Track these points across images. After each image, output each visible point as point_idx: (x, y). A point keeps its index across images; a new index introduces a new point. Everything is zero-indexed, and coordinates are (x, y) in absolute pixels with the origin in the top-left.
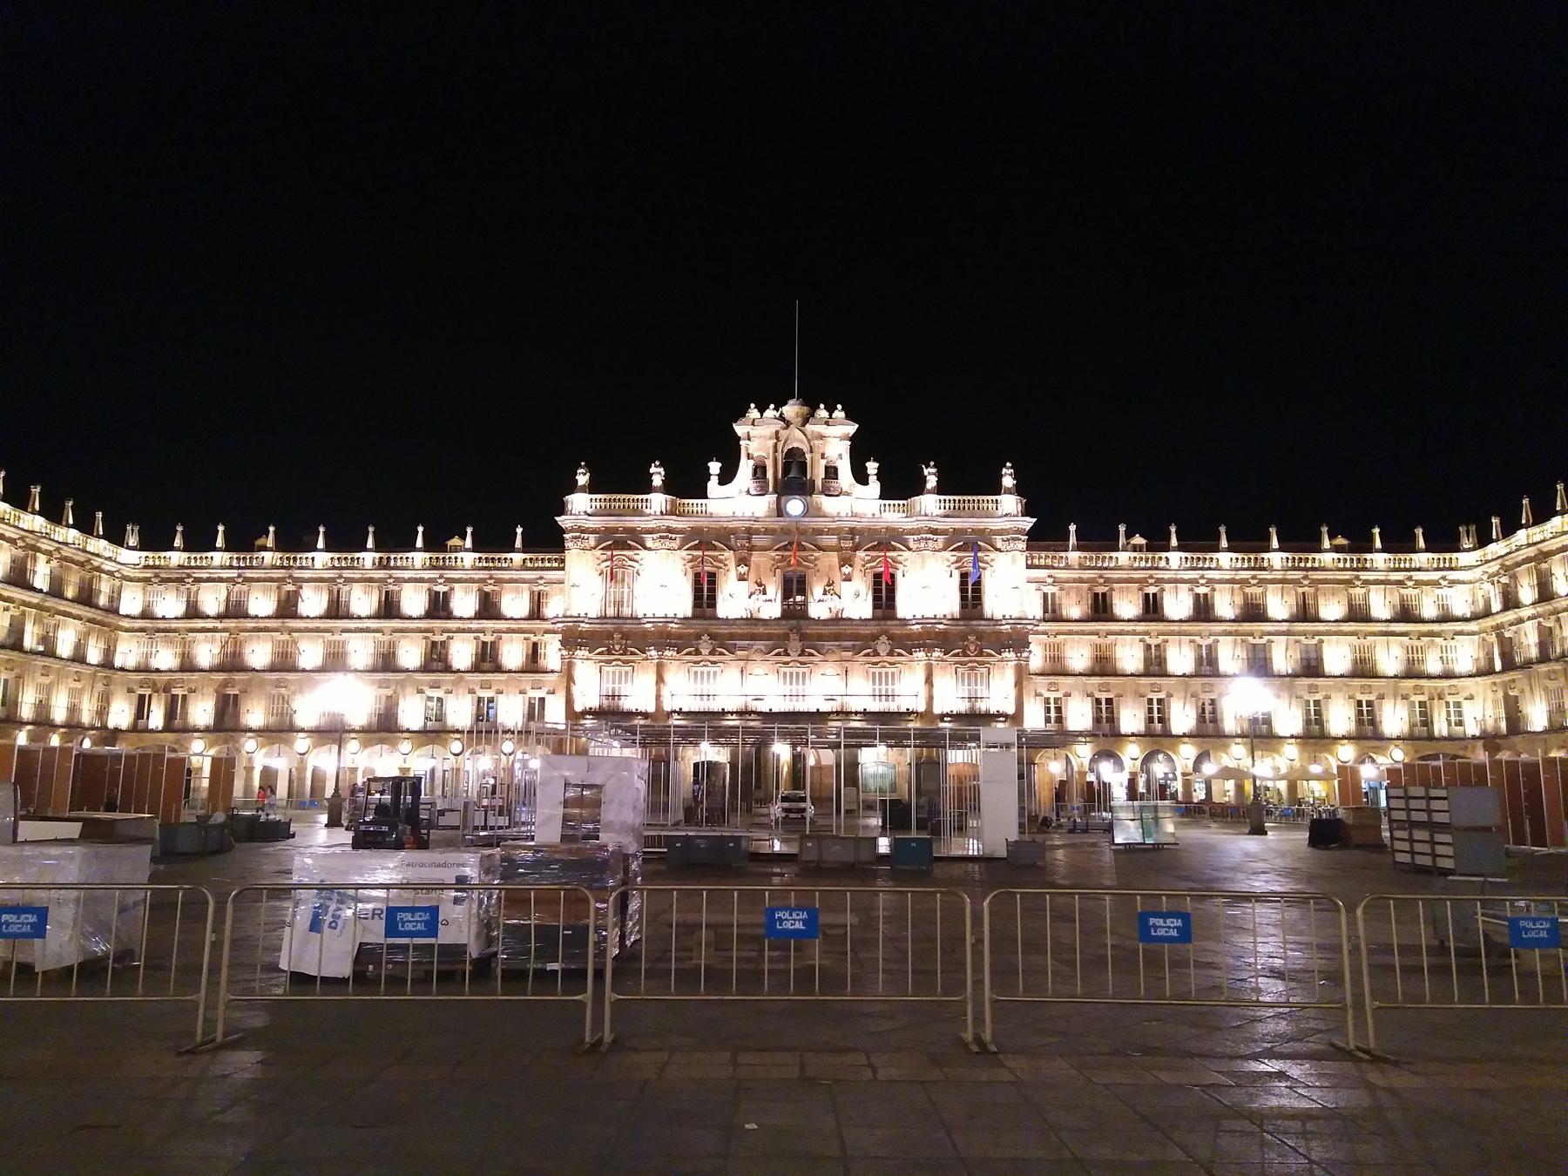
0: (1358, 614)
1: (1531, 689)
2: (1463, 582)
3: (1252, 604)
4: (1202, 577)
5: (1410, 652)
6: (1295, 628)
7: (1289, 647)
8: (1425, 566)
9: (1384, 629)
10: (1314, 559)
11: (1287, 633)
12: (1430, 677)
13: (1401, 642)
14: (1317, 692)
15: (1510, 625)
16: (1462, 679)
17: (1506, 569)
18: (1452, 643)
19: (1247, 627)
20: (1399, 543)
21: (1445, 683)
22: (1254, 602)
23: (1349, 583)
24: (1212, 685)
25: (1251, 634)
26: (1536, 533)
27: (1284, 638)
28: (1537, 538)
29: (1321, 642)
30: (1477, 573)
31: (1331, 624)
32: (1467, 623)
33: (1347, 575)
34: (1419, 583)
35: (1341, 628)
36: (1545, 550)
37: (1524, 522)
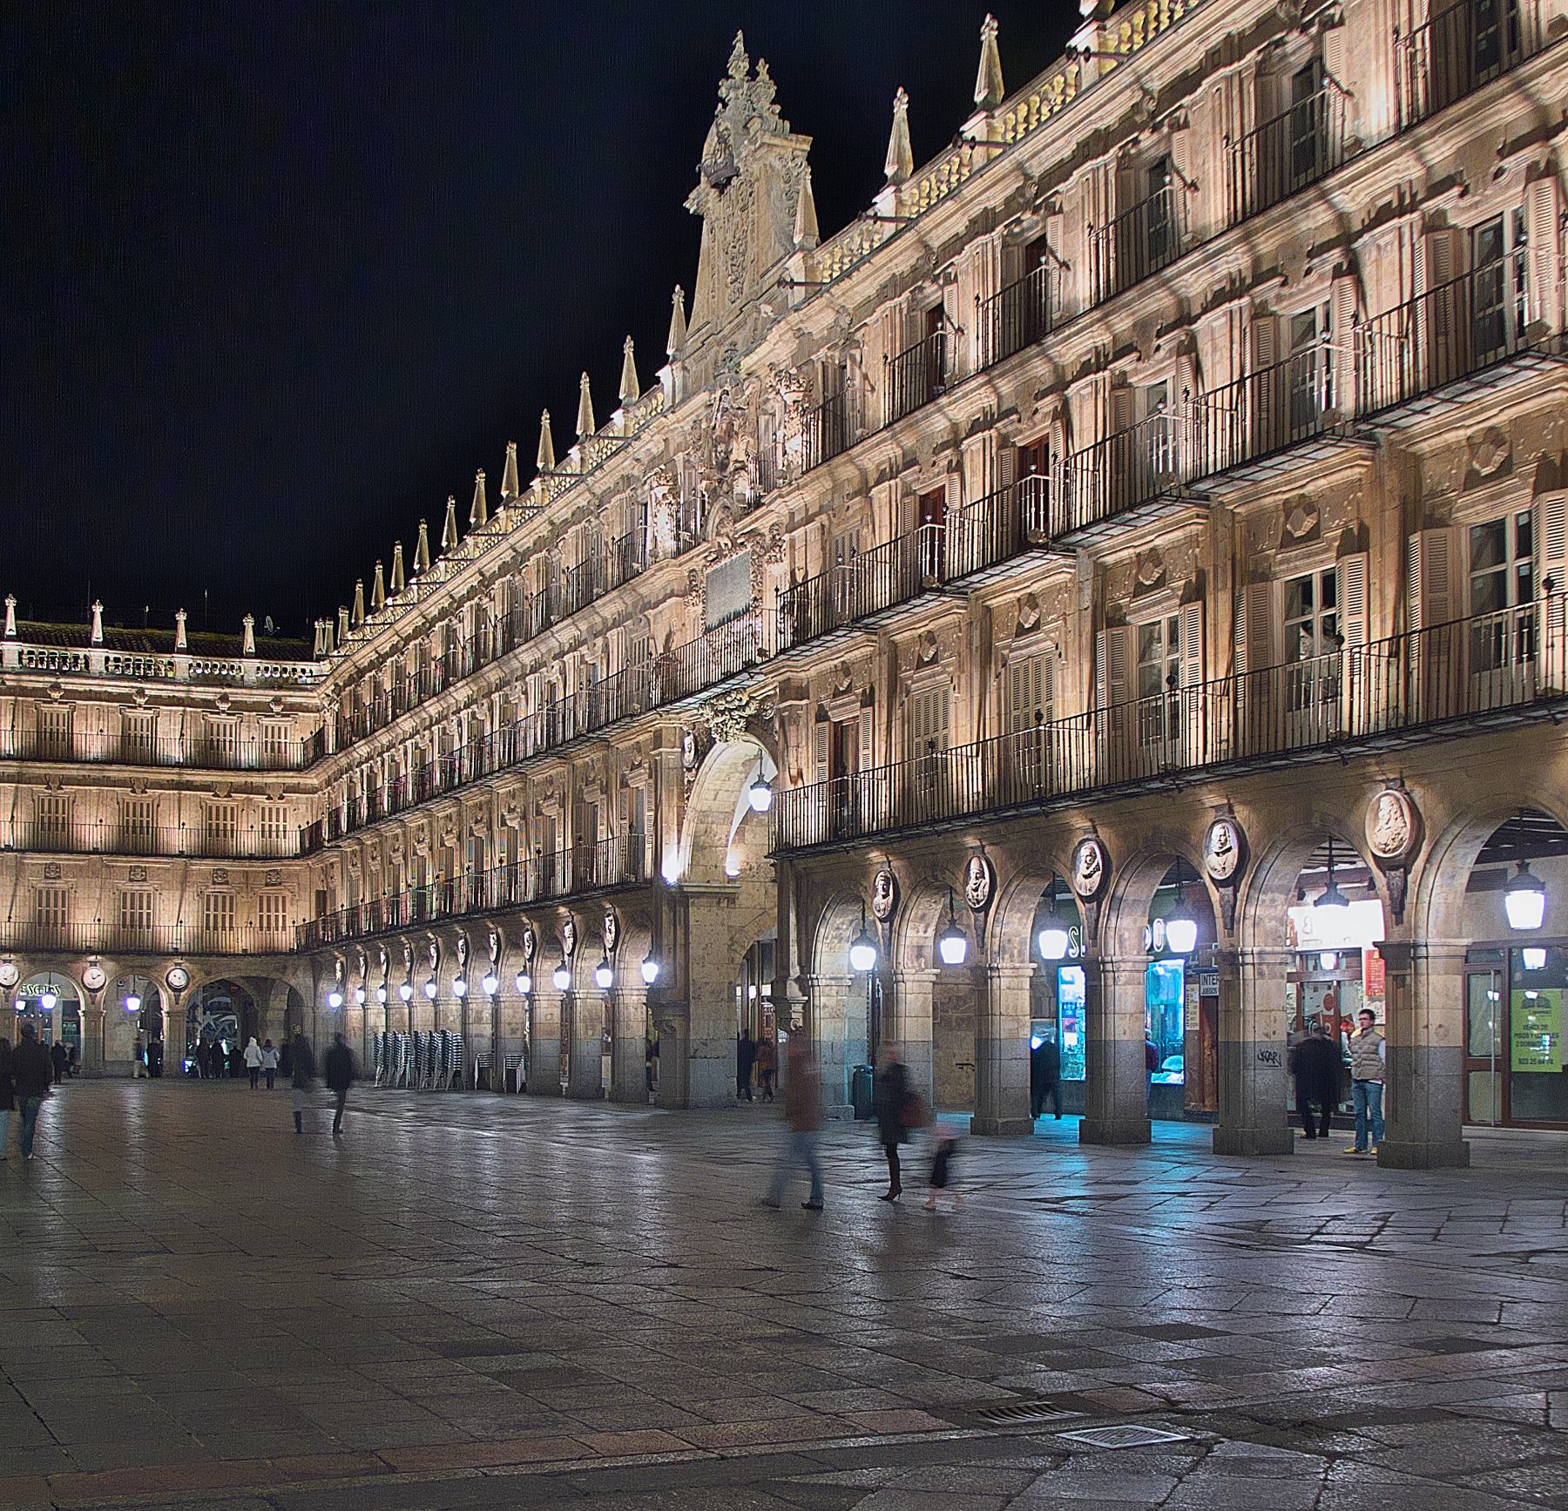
2: (307, 709)
5: (214, 816)
6: (37, 771)
9: (175, 777)
10: (76, 658)
11: (18, 779)
12: (238, 857)
14: (59, 877)
16: (286, 862)
18: (281, 805)
21: (257, 867)
27: (11, 786)
31: (88, 766)
32: (302, 774)
33: (124, 687)
34: (238, 707)
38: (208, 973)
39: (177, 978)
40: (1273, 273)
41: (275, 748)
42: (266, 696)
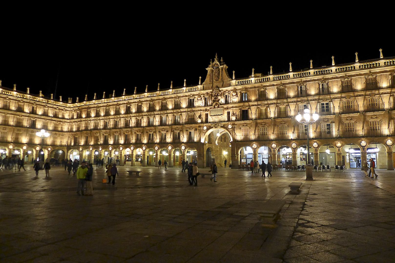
0: (45, 114)
1: (81, 136)
3: (20, 107)
4: (7, 97)
7: (28, 120)
8: (61, 105)
9: (51, 119)
13: (54, 122)
15: (78, 122)
17: (79, 109)
18: (64, 124)
19: (18, 113)
20: (57, 99)
21: (61, 133)
22: (21, 107)
23: (44, 106)
24: (6, 128)
25: (19, 115)
26: (88, 103)
27: (27, 118)
28: (88, 104)
29: (36, 120)
30: (72, 109)
33: (44, 104)
35: (42, 117)
36: (90, 107)
37: (85, 100)
38: (53, 148)
39: (49, 149)
40: (323, 100)
41: (63, 116)
42: (63, 108)
